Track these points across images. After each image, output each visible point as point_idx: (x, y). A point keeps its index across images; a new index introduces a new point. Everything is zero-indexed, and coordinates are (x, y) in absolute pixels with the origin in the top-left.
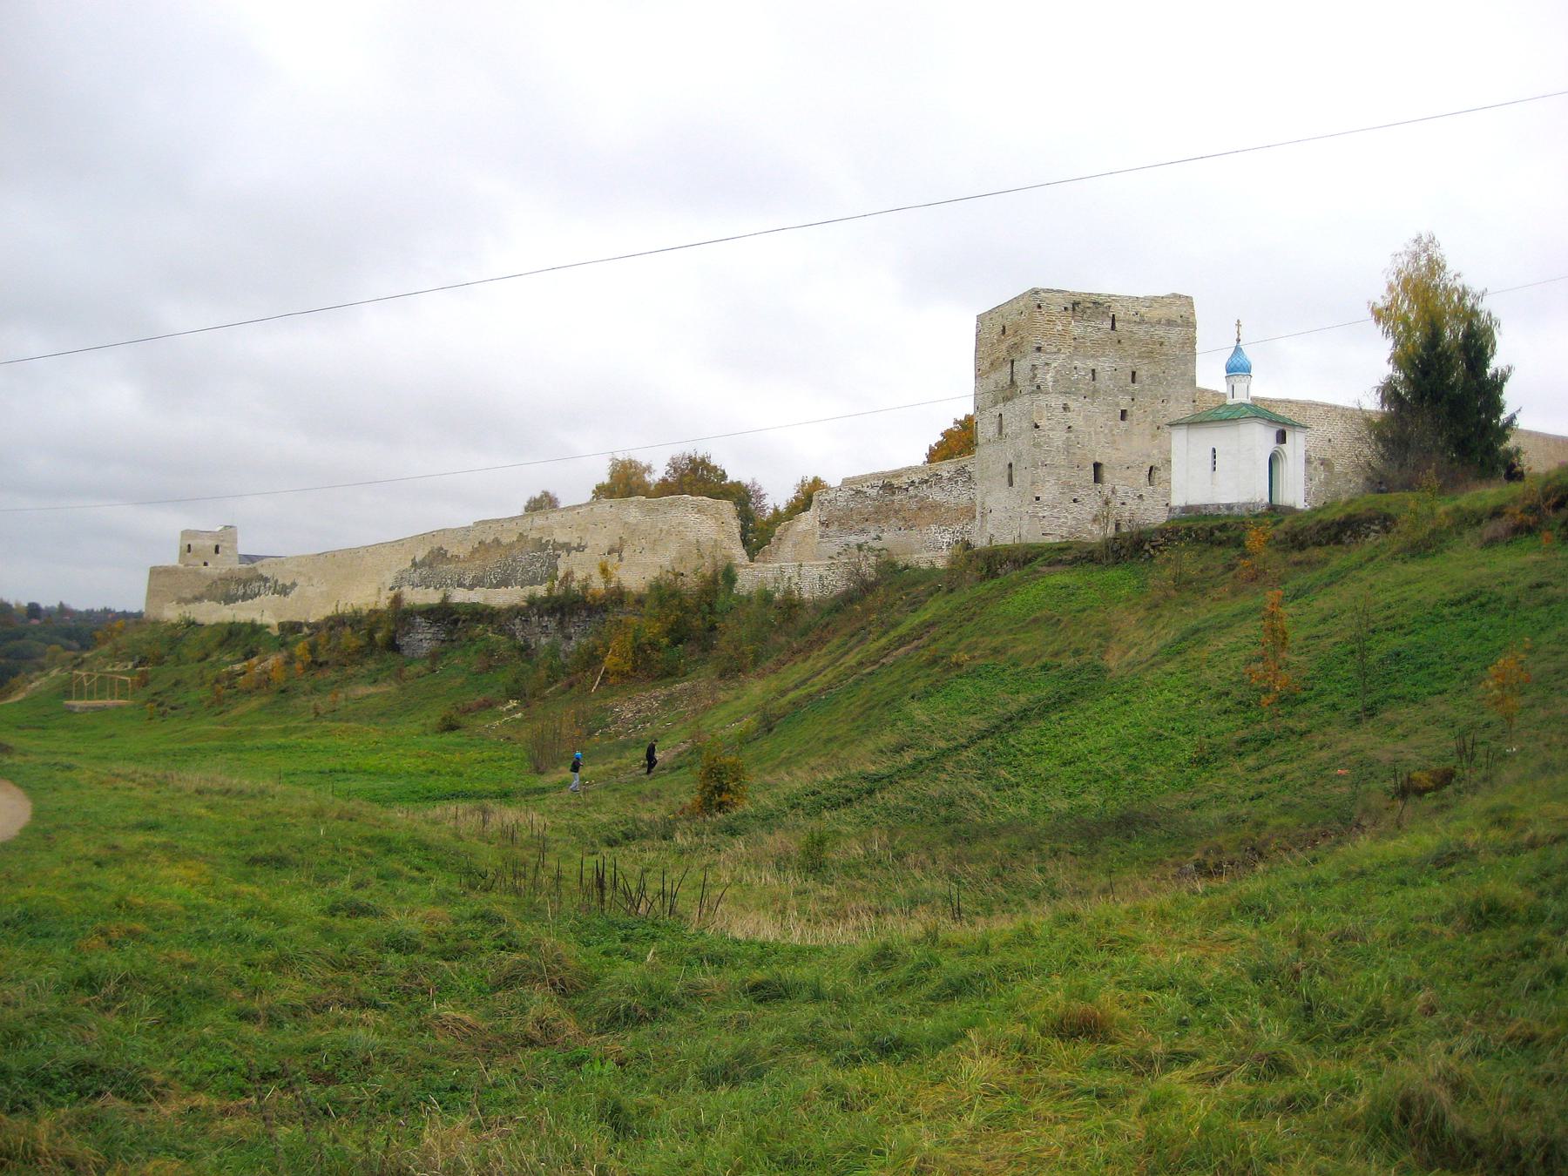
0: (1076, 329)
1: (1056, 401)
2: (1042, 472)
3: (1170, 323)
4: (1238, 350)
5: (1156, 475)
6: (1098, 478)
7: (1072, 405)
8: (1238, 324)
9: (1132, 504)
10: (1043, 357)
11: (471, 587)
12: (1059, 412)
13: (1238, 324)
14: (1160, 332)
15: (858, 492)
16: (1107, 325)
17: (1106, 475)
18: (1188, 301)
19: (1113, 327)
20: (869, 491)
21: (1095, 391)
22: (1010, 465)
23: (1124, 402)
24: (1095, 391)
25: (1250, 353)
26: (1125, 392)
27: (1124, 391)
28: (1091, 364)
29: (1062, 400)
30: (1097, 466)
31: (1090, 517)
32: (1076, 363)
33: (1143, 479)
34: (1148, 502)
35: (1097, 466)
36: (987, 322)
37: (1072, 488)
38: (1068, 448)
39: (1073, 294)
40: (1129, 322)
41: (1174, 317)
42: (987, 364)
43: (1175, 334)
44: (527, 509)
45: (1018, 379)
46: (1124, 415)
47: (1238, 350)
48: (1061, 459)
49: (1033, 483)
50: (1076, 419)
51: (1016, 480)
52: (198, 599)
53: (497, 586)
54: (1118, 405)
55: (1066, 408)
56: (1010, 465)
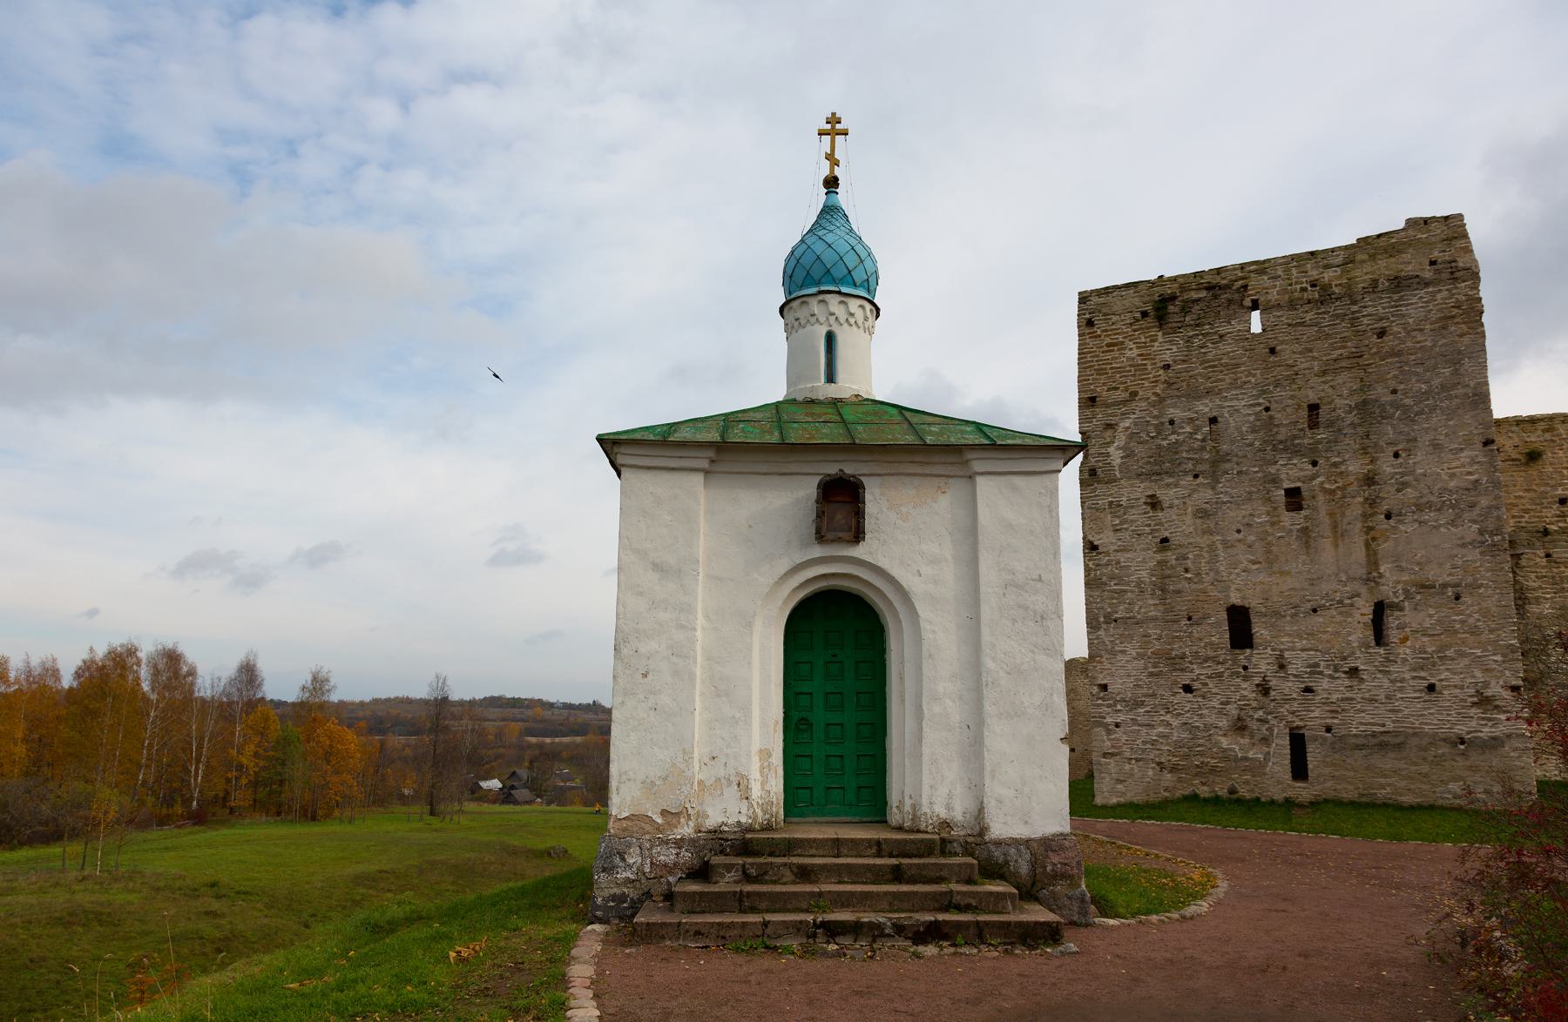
0: (1165, 348)
1: (1137, 491)
3: (1399, 283)
4: (830, 212)
5: (1392, 621)
7: (1166, 495)
9: (1331, 687)
10: (1101, 415)
13: (833, 128)
14: (1375, 308)
17: (1260, 631)
23: (1292, 472)
24: (1219, 460)
26: (1296, 452)
28: (1205, 407)
29: (1141, 490)
31: (1224, 723)
34: (1374, 684)
37: (1175, 662)
38: (1162, 586)
39: (1151, 284)
40: (1292, 305)
41: (1409, 269)
43: (1416, 305)
46: (1294, 499)
48: (1149, 606)
50: (1181, 526)
54: (1275, 481)
55: (1154, 503)
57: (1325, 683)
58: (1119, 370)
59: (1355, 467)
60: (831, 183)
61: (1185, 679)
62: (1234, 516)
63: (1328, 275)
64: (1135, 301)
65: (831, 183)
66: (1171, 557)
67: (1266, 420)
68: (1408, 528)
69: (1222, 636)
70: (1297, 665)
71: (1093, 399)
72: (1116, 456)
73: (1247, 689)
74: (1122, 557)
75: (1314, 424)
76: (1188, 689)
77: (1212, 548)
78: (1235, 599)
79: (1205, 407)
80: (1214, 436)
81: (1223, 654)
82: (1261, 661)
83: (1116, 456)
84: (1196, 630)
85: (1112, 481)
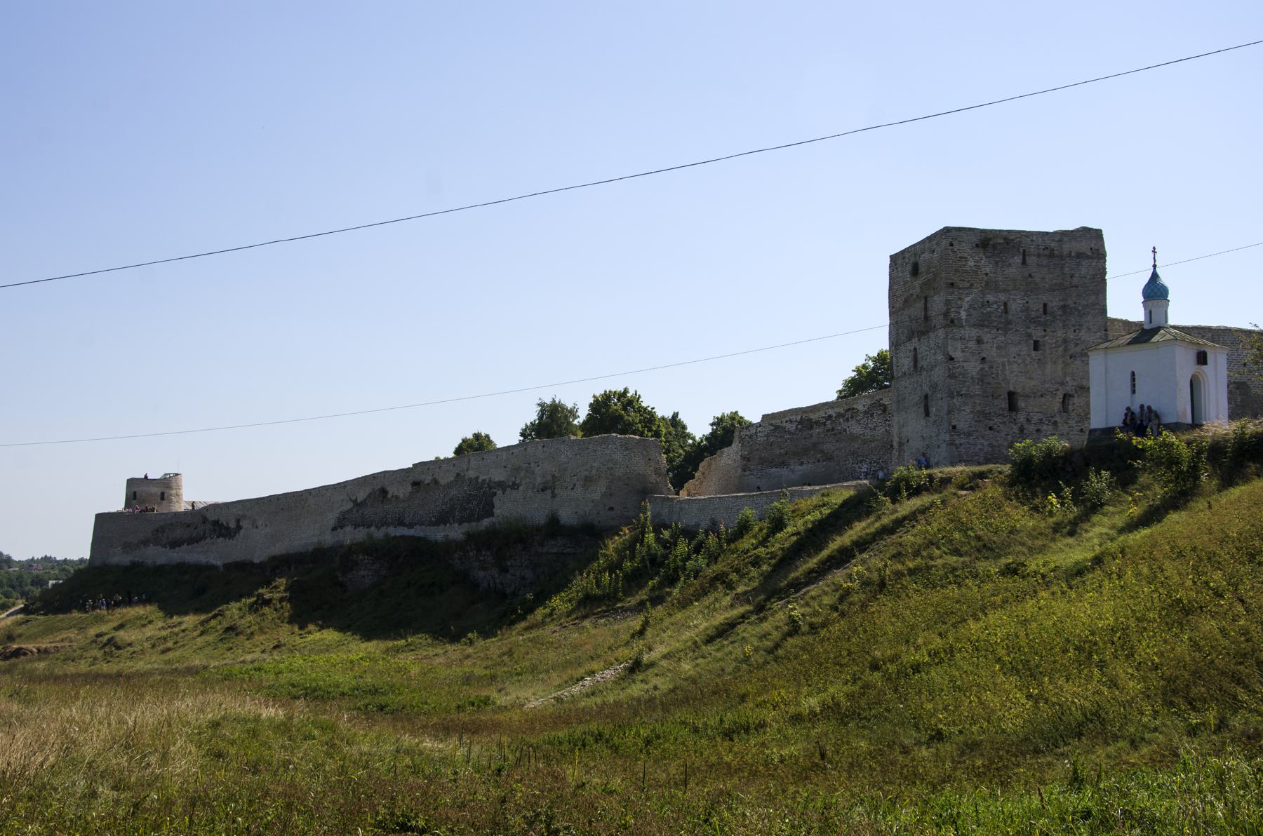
2: (957, 401)
4: (1155, 276)
6: (1013, 407)
7: (987, 337)
8: (1154, 252)
11: (411, 526)
12: (972, 344)
15: (777, 428)
16: (1018, 260)
17: (1021, 404)
18: (1096, 235)
19: (1024, 263)
20: (788, 426)
21: (1008, 322)
22: (926, 397)
24: (1008, 322)
25: (1165, 278)
27: (1035, 321)
28: (1002, 297)
29: (974, 332)
30: (1011, 395)
32: (990, 298)
33: (1057, 405)
35: (1011, 395)
36: (900, 261)
37: (987, 416)
38: (982, 379)
42: (901, 301)
43: (1085, 268)
44: (459, 451)
45: (932, 313)
46: (1036, 346)
47: (1155, 276)
48: (976, 390)
49: (949, 412)
50: (991, 352)
51: (933, 410)
52: (145, 543)
53: (437, 523)
54: (1030, 336)
56: (926, 397)
57: (1045, 427)
58: (966, 272)
59: (1060, 334)
60: (1155, 266)
61: (991, 423)
62: (1013, 350)
63: (1053, 245)
64: (975, 240)
65: (1155, 266)
66: (986, 366)
67: (1026, 309)
68: (1078, 362)
69: (1005, 405)
70: (1035, 419)
71: (952, 284)
72: (963, 314)
73: (1016, 429)
74: (965, 364)
75: (1045, 312)
76: (991, 428)
77: (1003, 365)
78: (1011, 389)
79: (1002, 297)
80: (1006, 311)
81: (1006, 413)
82: (1021, 417)
83: (963, 314)
84: (996, 402)
85: (962, 326)
